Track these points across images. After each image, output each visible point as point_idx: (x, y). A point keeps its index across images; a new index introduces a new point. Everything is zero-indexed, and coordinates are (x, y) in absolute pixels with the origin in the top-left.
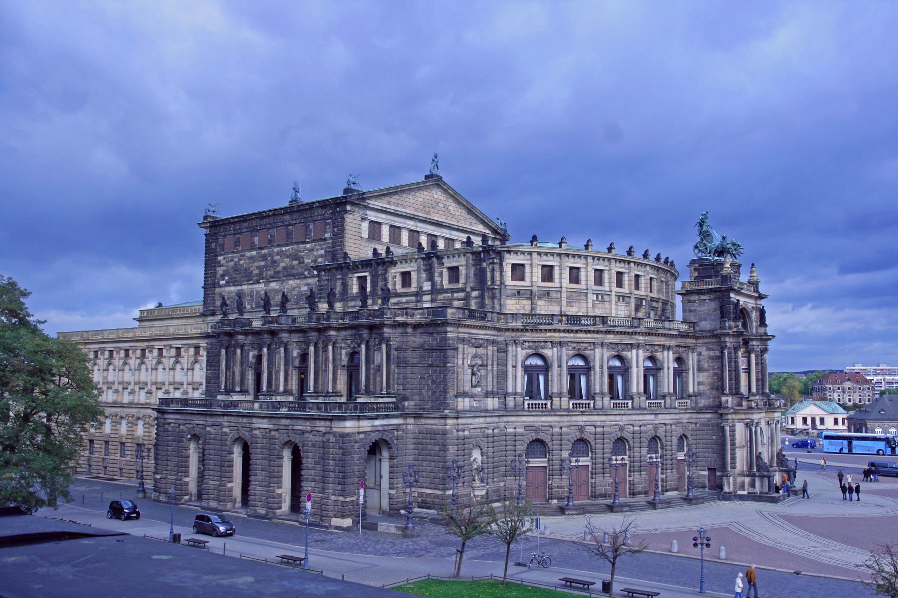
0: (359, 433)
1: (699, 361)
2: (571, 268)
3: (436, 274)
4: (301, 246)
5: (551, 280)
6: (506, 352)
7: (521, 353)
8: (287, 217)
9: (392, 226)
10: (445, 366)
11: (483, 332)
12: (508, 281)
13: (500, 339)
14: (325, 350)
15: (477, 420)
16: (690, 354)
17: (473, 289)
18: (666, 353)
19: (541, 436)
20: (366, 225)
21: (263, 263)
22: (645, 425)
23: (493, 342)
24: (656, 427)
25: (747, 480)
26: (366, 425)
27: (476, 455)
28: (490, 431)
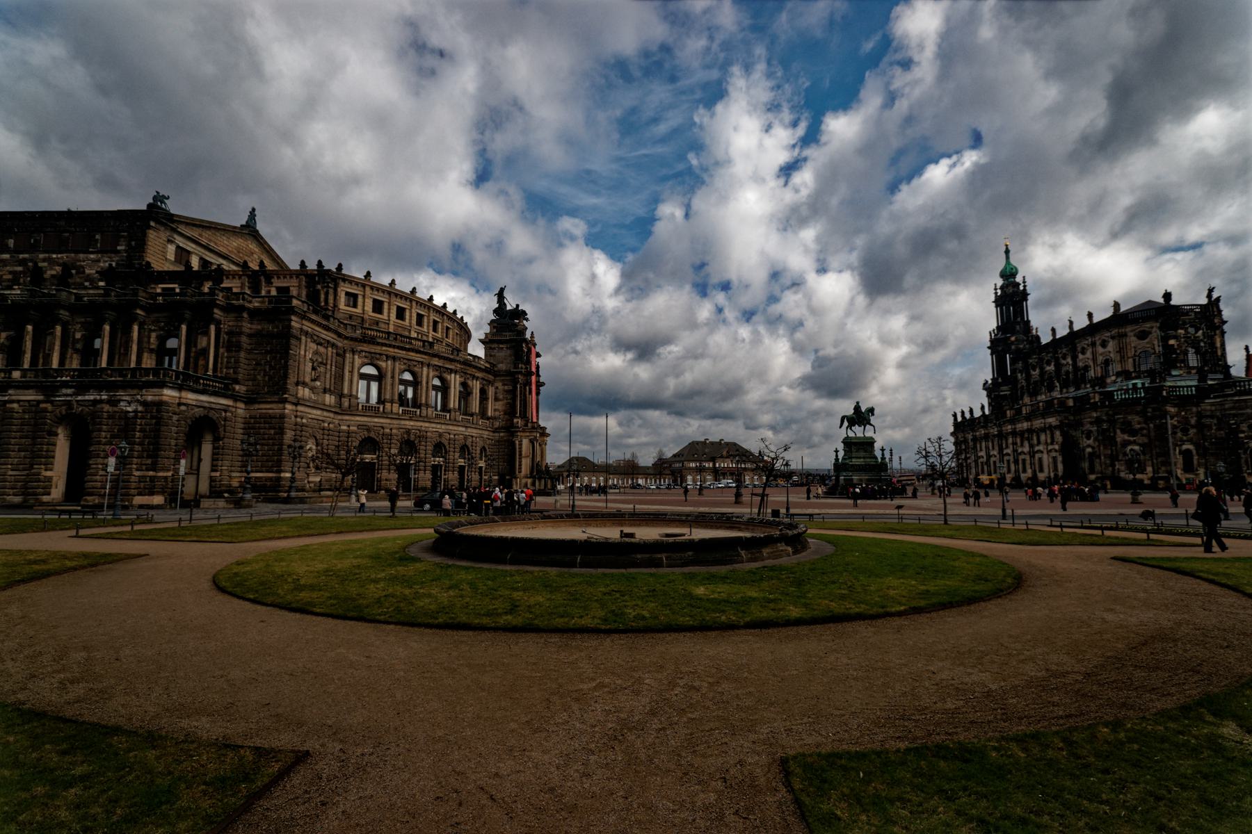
4: (82, 256)
5: (381, 312)
6: (344, 357)
8: (63, 223)
9: (201, 259)
10: (288, 353)
12: (342, 306)
13: (340, 344)
14: (128, 332)
15: (315, 412)
19: (372, 435)
20: (171, 248)
21: (20, 269)
23: (333, 345)
24: (466, 438)
25: (529, 481)
26: (190, 397)
27: (311, 445)
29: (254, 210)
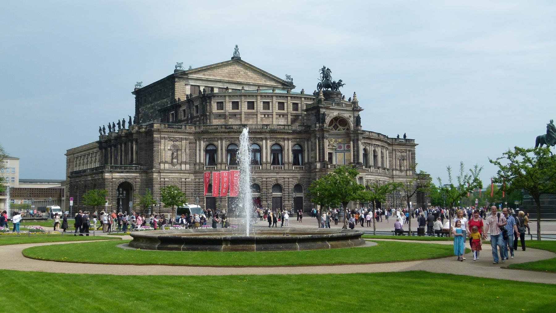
0: (112, 178)
1: (312, 146)
2: (248, 102)
3: (192, 110)
7: (203, 144)
8: (159, 86)
10: (153, 150)
11: (178, 134)
13: (190, 137)
15: (174, 174)
16: (306, 142)
17: (201, 116)
18: (286, 142)
20: (188, 88)
22: (270, 178)
26: (117, 175)
28: (184, 180)
29: (237, 47)
